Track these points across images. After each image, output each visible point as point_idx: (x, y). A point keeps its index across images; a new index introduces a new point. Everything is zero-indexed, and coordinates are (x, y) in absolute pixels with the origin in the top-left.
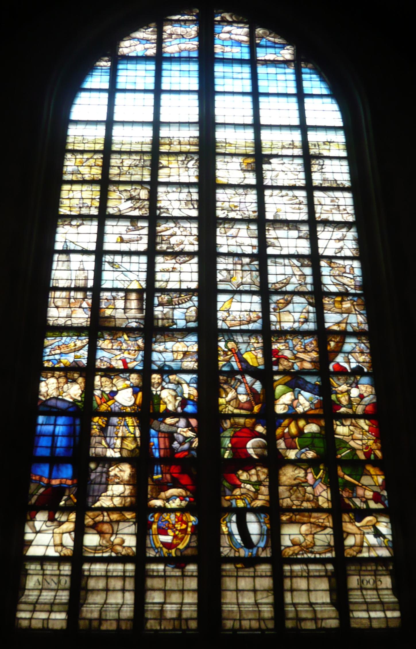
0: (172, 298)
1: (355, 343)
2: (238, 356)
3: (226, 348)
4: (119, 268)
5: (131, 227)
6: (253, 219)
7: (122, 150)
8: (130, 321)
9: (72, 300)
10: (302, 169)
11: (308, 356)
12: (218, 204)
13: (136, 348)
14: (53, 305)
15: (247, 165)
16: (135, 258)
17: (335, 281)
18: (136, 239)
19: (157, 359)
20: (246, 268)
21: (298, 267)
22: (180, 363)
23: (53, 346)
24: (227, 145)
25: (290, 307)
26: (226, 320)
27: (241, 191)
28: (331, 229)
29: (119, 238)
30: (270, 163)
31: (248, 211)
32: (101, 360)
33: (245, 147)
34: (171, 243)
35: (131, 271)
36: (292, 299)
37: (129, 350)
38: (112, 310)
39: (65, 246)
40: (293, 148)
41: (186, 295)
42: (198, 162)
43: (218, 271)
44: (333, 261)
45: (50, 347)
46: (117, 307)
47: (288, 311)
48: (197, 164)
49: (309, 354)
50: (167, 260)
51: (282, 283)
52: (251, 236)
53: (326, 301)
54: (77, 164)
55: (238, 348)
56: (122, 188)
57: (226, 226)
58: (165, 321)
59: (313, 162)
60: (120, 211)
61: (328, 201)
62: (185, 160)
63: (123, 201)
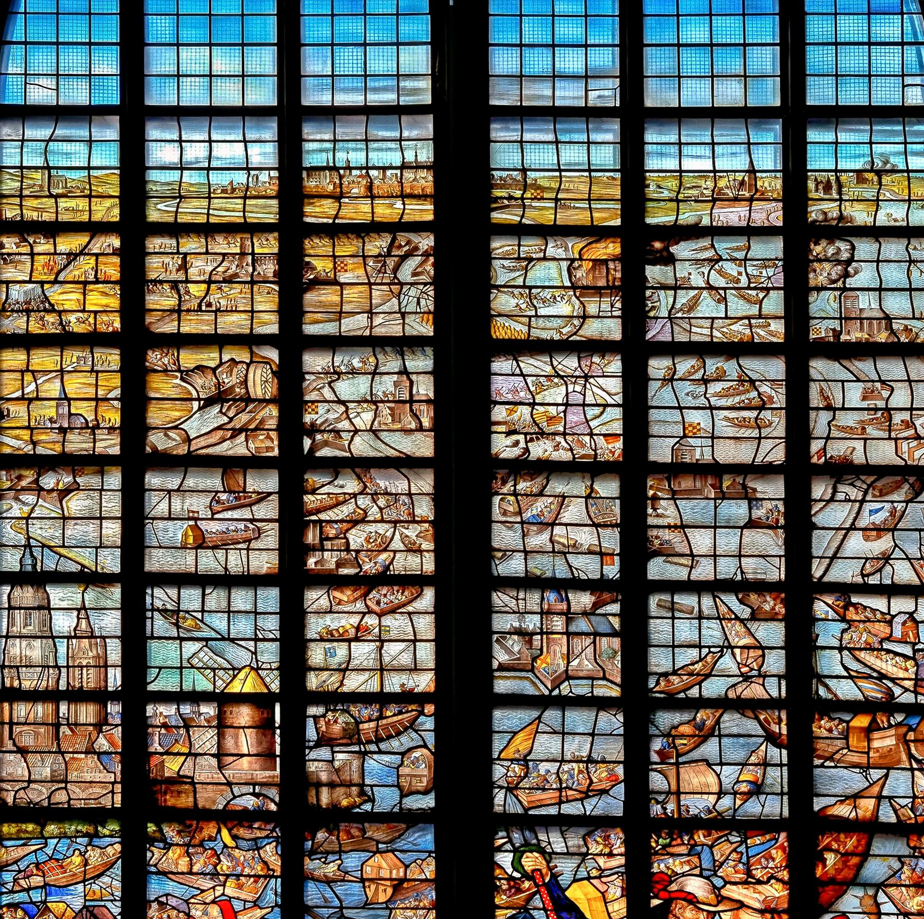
0: (357, 723)
1: (900, 858)
2: (550, 894)
3: (515, 869)
4: (199, 629)
5: (223, 497)
6: (607, 462)
7: (182, 219)
8: (236, 790)
9: (64, 730)
10: (779, 280)
11: (757, 895)
12: (499, 413)
13: (259, 869)
14: (9, 745)
15: (593, 268)
16: (242, 599)
17: (854, 666)
18: (245, 535)
19: (320, 902)
20: (582, 625)
21: (742, 621)
22: (388, 912)
23: (22, 865)
24: (528, 195)
25: (710, 748)
26: (516, 787)
27: (569, 363)
28: (855, 494)
29: (190, 533)
30: (670, 260)
31: (591, 435)
32: (161, 904)
33: (589, 200)
34: (352, 548)
35: (233, 640)
36: (718, 722)
37: (238, 876)
38: (183, 758)
39: (29, 561)
40: (751, 200)
41: (400, 713)
42: (432, 259)
43: (495, 637)
44: (854, 600)
45: (15, 867)
46: (197, 749)
47: (706, 761)
48: (429, 268)
49: (759, 887)
50: (339, 604)
51: (691, 674)
52: (599, 520)
53: (822, 727)
54: (37, 277)
55: (550, 869)
56: (189, 358)
57: (522, 486)
58: (340, 791)
59: (817, 250)
60: (188, 440)
61: (854, 395)
62: (389, 254)
63: (195, 405)
